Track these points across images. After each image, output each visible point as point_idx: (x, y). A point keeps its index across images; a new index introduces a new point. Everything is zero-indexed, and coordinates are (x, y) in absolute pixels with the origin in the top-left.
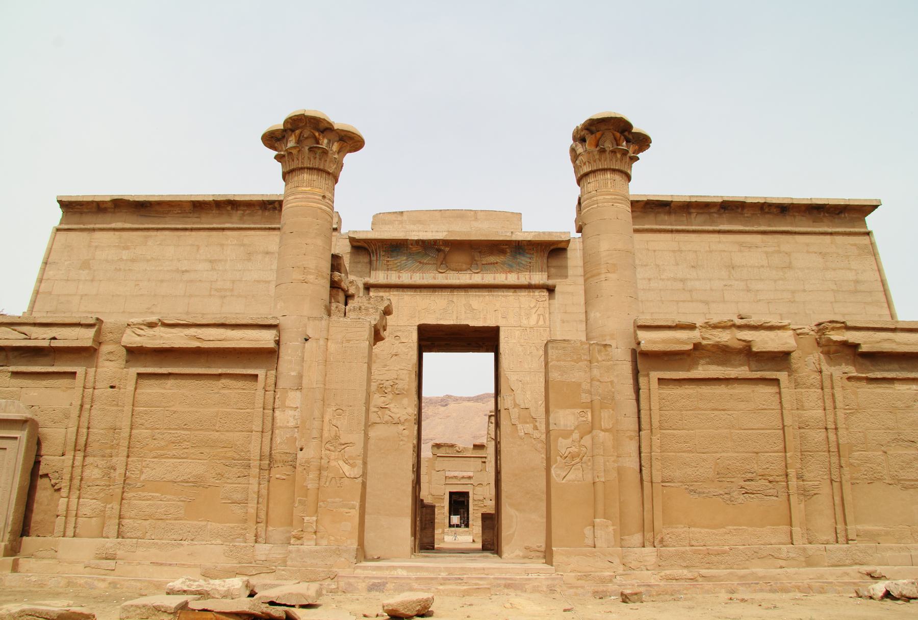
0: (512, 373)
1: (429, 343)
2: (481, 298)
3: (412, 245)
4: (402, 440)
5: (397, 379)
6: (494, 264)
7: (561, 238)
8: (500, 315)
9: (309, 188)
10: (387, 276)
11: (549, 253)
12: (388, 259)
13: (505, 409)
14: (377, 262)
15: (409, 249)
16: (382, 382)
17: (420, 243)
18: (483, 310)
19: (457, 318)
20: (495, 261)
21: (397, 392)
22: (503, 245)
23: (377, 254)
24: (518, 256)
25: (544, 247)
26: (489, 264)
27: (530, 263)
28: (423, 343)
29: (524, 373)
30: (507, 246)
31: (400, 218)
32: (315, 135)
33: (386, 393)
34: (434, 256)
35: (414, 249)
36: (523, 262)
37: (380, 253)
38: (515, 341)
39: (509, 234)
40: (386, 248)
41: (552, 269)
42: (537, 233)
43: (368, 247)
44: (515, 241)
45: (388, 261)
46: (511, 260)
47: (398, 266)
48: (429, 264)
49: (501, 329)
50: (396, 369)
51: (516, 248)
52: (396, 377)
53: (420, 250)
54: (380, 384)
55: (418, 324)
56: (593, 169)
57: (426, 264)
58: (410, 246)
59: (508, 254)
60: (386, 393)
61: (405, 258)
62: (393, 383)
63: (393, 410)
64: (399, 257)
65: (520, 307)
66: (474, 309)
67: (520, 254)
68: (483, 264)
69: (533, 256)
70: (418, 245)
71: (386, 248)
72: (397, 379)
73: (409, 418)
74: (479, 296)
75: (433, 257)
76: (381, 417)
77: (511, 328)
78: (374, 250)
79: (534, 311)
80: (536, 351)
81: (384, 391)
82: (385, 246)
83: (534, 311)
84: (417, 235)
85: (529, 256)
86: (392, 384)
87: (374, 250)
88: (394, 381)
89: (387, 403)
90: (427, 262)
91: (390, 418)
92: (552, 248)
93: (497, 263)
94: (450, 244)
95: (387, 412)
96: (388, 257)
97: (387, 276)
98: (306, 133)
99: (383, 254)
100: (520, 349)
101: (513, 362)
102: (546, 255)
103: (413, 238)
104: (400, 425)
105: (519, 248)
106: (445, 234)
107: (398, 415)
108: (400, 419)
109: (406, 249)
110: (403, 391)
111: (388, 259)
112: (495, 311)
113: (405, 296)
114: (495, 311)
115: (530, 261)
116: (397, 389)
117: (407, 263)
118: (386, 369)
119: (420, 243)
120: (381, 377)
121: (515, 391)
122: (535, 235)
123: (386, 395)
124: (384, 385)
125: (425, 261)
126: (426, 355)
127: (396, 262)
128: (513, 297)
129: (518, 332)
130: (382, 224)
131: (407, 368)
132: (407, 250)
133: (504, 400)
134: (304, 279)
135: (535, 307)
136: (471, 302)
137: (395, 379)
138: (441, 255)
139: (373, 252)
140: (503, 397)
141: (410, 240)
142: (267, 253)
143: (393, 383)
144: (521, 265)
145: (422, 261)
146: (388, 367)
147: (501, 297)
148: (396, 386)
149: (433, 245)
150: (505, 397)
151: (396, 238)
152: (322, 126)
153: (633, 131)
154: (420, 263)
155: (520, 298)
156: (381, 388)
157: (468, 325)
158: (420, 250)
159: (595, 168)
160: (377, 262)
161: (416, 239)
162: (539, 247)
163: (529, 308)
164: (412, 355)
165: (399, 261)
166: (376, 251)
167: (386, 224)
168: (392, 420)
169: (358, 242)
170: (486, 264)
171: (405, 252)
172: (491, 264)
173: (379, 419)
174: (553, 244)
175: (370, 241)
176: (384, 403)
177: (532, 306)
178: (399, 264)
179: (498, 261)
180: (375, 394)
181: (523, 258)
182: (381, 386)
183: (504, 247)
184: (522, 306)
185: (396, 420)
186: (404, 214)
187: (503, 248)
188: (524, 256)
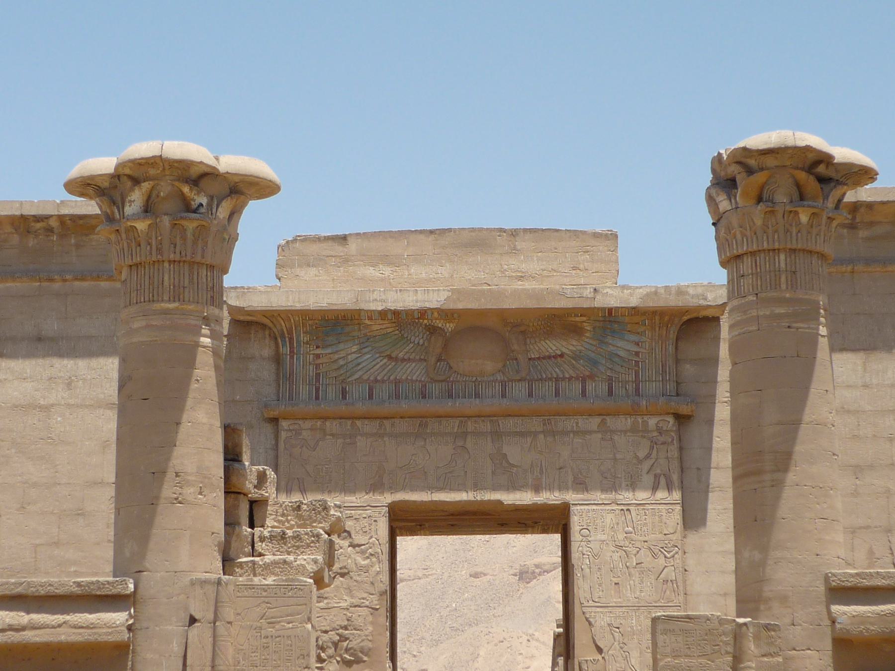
1: (414, 524)
2: (529, 440)
3: (370, 319)
6: (555, 357)
7: (705, 299)
8: (570, 478)
9: (176, 304)
10: (317, 390)
11: (680, 330)
12: (318, 351)
14: (292, 357)
17: (390, 317)
18: (532, 465)
20: (559, 353)
22: (576, 316)
23: (291, 339)
24: (609, 340)
25: (666, 318)
26: (544, 358)
27: (637, 354)
28: (395, 524)
30: (584, 319)
31: (339, 249)
32: (183, 194)
34: (421, 342)
35: (375, 327)
36: (622, 353)
37: (298, 336)
38: (604, 537)
39: (588, 292)
41: (688, 366)
42: (653, 290)
43: (271, 325)
44: (603, 309)
45: (318, 356)
47: (342, 366)
48: (409, 360)
49: (572, 508)
53: (389, 330)
56: (750, 250)
57: (403, 360)
58: (367, 322)
59: (587, 335)
64: (341, 346)
65: (615, 459)
66: (513, 466)
68: (530, 359)
69: (644, 339)
74: (522, 434)
75: (418, 343)
77: (594, 507)
78: (285, 330)
79: (646, 466)
80: (650, 558)
82: (310, 322)
83: (646, 466)
84: (381, 301)
87: (285, 330)
92: (685, 318)
93: (562, 356)
94: (455, 315)
96: (318, 347)
97: (317, 390)
98: (165, 189)
100: (616, 556)
102: (673, 335)
103: (373, 307)
106: (443, 296)
109: (356, 327)
111: (318, 351)
112: (560, 469)
113: (359, 437)
114: (560, 469)
115: (636, 349)
117: (360, 360)
119: (390, 317)
121: (605, 650)
122: (648, 295)
125: (401, 355)
126: (405, 544)
127: (336, 356)
128: (600, 436)
129: (611, 516)
130: (300, 266)
131: (367, 603)
132: (360, 330)
134: (175, 496)
135: (648, 457)
136: (506, 449)
139: (283, 336)
141: (367, 311)
142: (39, 339)
144: (616, 359)
145: (394, 355)
147: (572, 435)
149: (418, 318)
152: (194, 172)
153: (835, 161)
154: (390, 357)
155: (616, 437)
159: (755, 248)
160: (292, 357)
161: (380, 308)
162: (657, 318)
163: (635, 461)
164: (378, 573)
166: (290, 332)
167: (309, 265)
169: (249, 315)
170: (539, 358)
172: (549, 357)
174: (687, 312)
175: (275, 315)
177: (641, 454)
178: (341, 362)
179: (564, 350)
181: (620, 344)
183: (578, 319)
184: (618, 456)
186: (349, 238)
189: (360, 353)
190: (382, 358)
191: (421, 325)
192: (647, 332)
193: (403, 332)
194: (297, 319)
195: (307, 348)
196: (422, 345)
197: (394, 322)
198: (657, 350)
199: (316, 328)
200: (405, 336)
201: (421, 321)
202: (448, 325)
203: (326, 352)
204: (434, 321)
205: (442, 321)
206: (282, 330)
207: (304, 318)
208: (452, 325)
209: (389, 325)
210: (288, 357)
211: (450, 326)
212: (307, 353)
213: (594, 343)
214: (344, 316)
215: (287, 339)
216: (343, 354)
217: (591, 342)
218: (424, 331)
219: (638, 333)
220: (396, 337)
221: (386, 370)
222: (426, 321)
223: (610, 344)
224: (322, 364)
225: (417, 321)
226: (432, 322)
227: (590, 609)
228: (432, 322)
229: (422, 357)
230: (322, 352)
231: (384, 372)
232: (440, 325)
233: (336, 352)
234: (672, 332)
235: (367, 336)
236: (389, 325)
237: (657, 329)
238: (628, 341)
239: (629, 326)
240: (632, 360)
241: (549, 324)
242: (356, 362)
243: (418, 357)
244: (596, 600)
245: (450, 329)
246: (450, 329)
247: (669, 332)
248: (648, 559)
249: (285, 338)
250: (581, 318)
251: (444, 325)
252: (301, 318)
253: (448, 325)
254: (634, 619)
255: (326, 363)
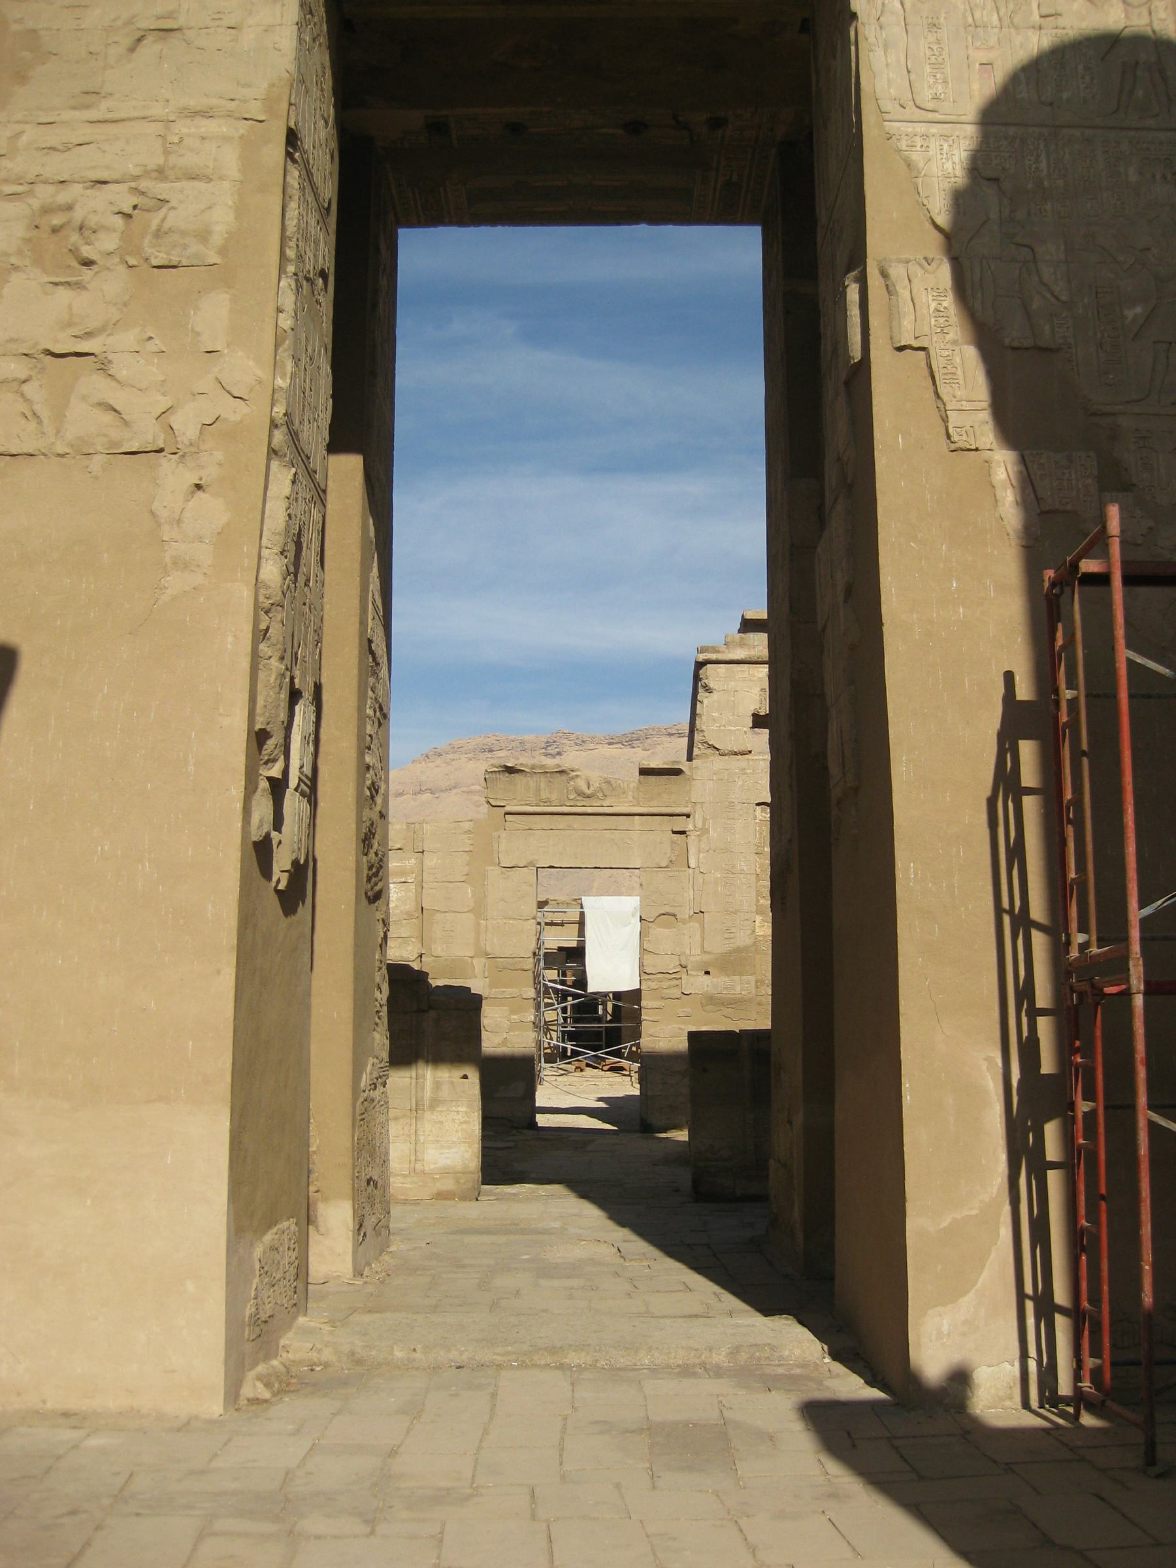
0: (934, 129)
4: (183, 564)
5: (161, 173)
13: (901, 349)
16: (63, 197)
21: (160, 258)
29: (1012, 131)
33: (88, 263)
50: (157, 110)
52: (158, 160)
54: (46, 210)
60: (88, 263)
62: (135, 200)
63: (123, 367)
72: (161, 173)
73: (234, 412)
76: (44, 413)
81: (74, 251)
88: (144, 184)
89: (92, 325)
91: (108, 418)
95: (94, 385)
101: (938, 66)
104: (166, 464)
107: (164, 403)
108: (176, 421)
110: (195, 247)
116: (158, 234)
120: (56, 166)
123: (87, 274)
124: (78, 215)
133: (890, 290)
137: (146, 174)
140: (884, 275)
143: (135, 200)
146: (104, 105)
148: (155, 220)
150: (897, 272)
156: (55, 230)
168: (114, 434)
173: (33, 425)
176: (70, 324)
180: (15, 268)
182: (57, 221)
185: (147, 434)
227: (909, 128)
244: (930, 106)
254: (1043, 158)
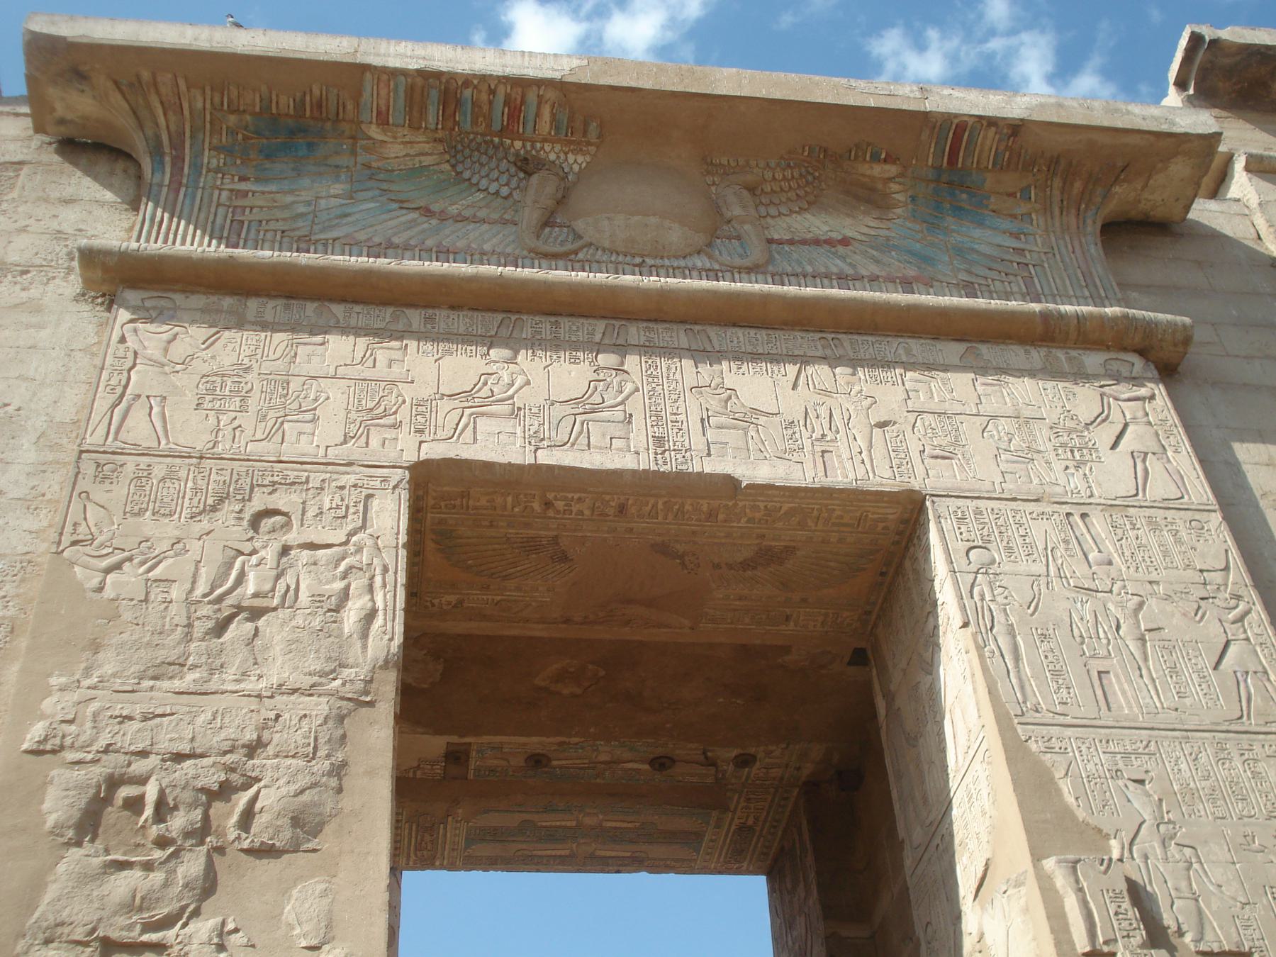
12: (243, 186)
15: (367, 150)
19: (659, 441)
22: (875, 158)
23: (178, 160)
24: (950, 222)
25: (1078, 185)
30: (892, 170)
37: (198, 155)
40: (232, 132)
46: (919, 236)
51: (937, 181)
53: (427, 161)
55: (410, 456)
58: (374, 132)
61: (338, 188)
64: (306, 182)
67: (958, 211)
69: (1027, 228)
70: (414, 127)
71: (232, 132)
75: (497, 193)
79: (1104, 435)
82: (233, 119)
83: (1104, 435)
85: (1007, 224)
86: (213, 779)
90: (467, 213)
96: (243, 179)
99: (210, 159)
105: (950, 183)
111: (243, 186)
118: (177, 684)
125: (453, 209)
129: (1044, 524)
132: (354, 153)
138: (541, 189)
145: (436, 207)
151: (304, 57)
157: (730, 483)
158: (427, 161)
162: (1057, 183)
165: (305, 195)
166: (177, 145)
171: (344, 160)
175: (146, 75)
181: (977, 233)
183: (878, 170)
187: (872, 178)
188: (981, 224)
189: (352, 198)
190: (404, 212)
191: (506, 150)
192: (1034, 216)
193: (460, 168)
194: (199, 105)
195: (215, 179)
196: (505, 198)
197: (441, 141)
198: (1063, 249)
199: (245, 138)
200: (467, 175)
201: (508, 142)
202: (571, 158)
203: (267, 189)
204: (538, 145)
205: (558, 147)
206: (158, 138)
207: (217, 99)
208: (580, 159)
209: (427, 148)
210: (165, 190)
211: (575, 160)
212: (214, 187)
213: (918, 227)
214: (320, 106)
215: (168, 159)
216: (305, 195)
217: (910, 225)
218: (513, 169)
219: (1014, 216)
220: (442, 177)
221: (416, 230)
222: (518, 144)
223: (953, 231)
224: (252, 208)
225: (496, 140)
226: (533, 147)
228: (533, 147)
229: (507, 217)
230: (254, 188)
231: (410, 233)
232: (552, 157)
233: (291, 192)
234: (1089, 221)
235: (370, 167)
236: (427, 148)
237: (1057, 211)
238: (990, 228)
239: (992, 200)
240: (1012, 262)
241: (810, 178)
242: (338, 212)
243: (495, 216)
245: (576, 168)
246: (576, 168)
247: (1084, 221)
248: (1175, 621)
249: (162, 155)
250: (887, 167)
251: (562, 156)
252: (208, 106)
253: (571, 158)
255: (261, 207)
